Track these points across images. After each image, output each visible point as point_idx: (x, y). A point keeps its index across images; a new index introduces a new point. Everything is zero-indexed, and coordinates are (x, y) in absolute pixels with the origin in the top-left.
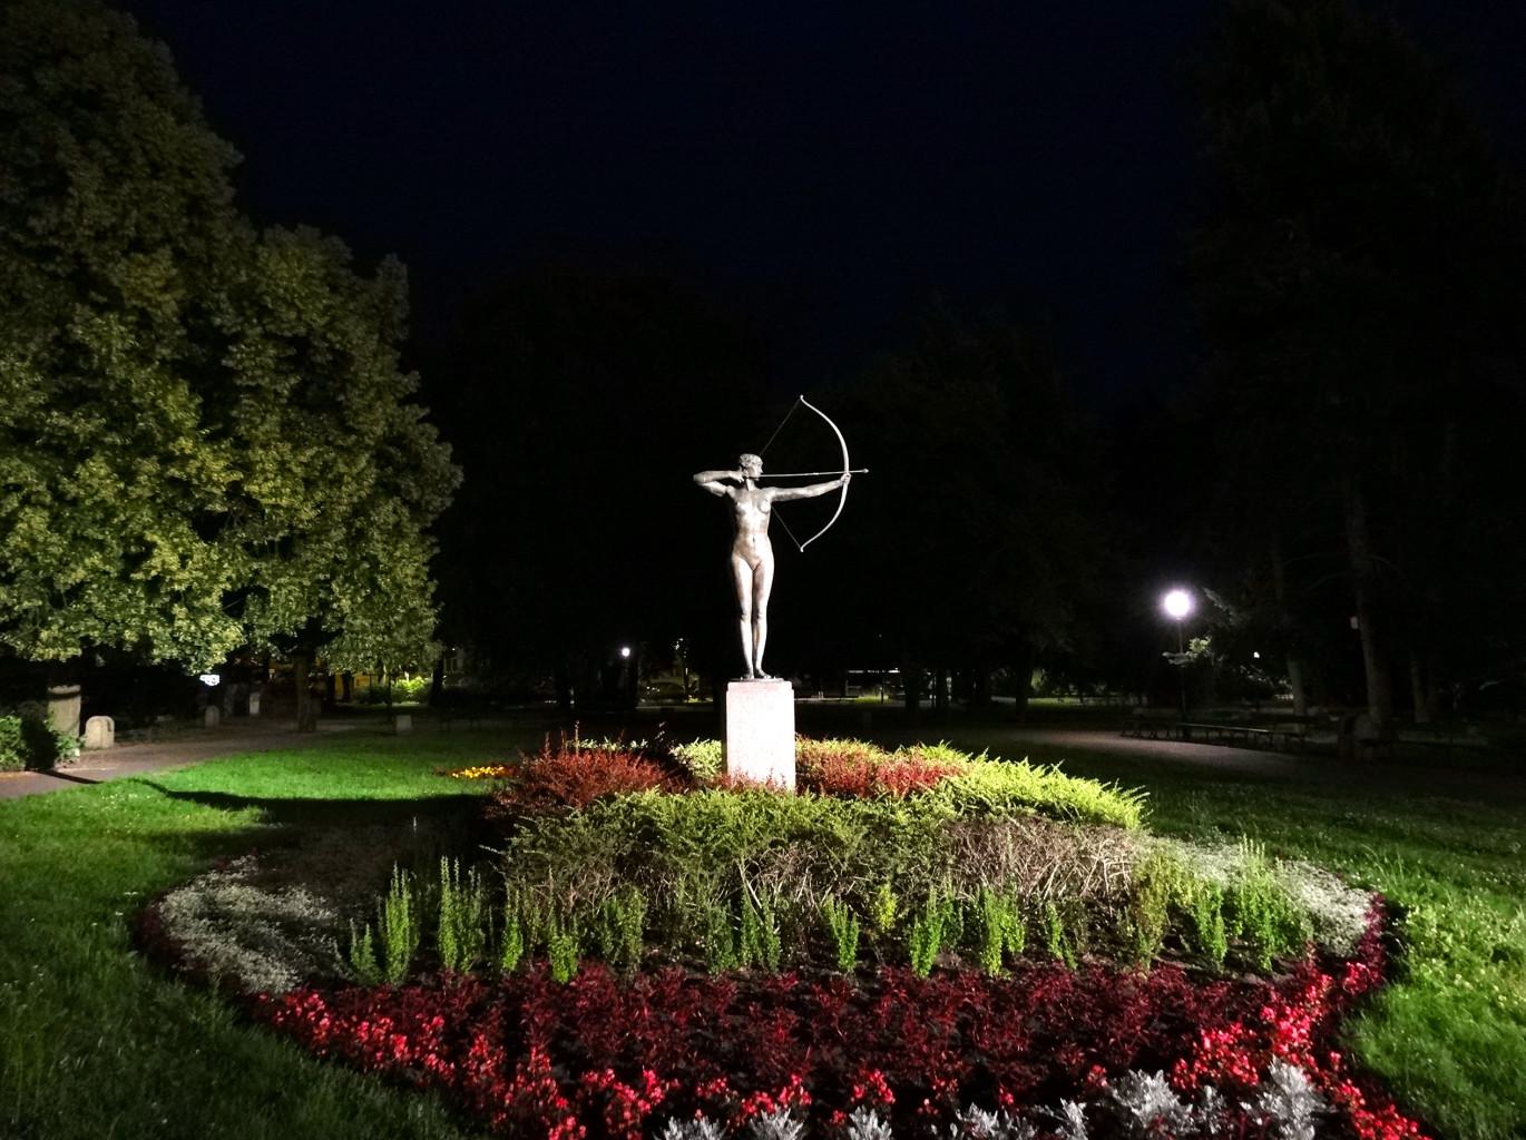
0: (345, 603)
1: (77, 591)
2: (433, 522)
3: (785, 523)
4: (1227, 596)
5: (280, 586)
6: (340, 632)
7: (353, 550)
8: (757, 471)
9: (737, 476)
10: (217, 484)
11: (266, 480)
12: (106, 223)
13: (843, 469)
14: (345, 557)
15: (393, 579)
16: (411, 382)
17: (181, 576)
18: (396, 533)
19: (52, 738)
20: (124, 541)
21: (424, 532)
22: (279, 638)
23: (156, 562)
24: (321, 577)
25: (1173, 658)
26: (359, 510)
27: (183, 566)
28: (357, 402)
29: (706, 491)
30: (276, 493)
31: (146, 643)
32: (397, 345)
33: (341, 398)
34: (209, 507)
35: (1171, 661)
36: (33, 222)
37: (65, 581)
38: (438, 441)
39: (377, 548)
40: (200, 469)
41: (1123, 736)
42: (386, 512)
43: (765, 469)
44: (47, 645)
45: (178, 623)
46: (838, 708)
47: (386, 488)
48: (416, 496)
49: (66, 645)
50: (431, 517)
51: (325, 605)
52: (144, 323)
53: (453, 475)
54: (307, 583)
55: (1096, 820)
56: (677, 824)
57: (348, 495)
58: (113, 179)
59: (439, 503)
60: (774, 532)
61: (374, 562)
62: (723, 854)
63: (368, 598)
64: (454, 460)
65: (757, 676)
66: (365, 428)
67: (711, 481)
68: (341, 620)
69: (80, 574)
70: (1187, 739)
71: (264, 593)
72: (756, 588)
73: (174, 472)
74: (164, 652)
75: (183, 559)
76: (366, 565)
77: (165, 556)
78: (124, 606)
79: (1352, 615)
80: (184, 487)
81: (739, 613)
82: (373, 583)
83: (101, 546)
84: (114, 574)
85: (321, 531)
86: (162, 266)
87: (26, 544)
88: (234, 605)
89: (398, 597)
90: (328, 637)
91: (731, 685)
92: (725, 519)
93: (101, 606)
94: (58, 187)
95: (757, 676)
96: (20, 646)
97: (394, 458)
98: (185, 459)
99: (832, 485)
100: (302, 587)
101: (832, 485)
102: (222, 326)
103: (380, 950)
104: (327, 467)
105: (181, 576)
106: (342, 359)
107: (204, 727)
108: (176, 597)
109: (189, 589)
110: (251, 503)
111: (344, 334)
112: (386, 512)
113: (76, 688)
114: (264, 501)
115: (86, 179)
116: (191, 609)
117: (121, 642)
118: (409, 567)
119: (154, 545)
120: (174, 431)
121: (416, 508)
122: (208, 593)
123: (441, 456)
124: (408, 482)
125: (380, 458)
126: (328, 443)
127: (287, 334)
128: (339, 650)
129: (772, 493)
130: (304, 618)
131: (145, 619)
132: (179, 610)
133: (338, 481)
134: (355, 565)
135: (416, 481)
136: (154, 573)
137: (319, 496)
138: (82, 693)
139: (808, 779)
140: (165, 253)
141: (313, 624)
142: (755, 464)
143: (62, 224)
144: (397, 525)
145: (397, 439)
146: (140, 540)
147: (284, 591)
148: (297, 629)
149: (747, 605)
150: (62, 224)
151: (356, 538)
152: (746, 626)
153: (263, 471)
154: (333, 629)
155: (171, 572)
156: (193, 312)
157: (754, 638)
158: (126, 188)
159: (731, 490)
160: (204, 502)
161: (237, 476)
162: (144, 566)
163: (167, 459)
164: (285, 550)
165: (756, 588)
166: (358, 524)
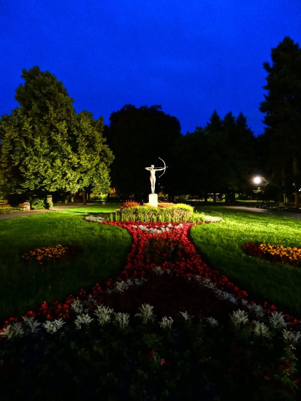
0: (96, 181)
1: (55, 181)
2: (110, 165)
3: (157, 174)
4: (266, 179)
5: (85, 178)
6: (95, 186)
7: (96, 172)
8: (153, 167)
9: (150, 168)
10: (76, 162)
11: (83, 161)
12: (55, 117)
13: (164, 167)
14: (95, 173)
15: (103, 177)
16: (105, 140)
17: (71, 178)
18: (104, 168)
19: (48, 204)
20: (62, 172)
21: (108, 167)
22: (85, 188)
23: (68, 176)
24: (92, 177)
25: (255, 191)
26: (98, 165)
27: (71, 176)
28: (97, 146)
29: (147, 170)
30: (85, 163)
31: (66, 188)
32: (102, 132)
33: (94, 145)
34: (75, 166)
35: (255, 192)
36: (44, 118)
37: (54, 179)
38: (110, 151)
39: (101, 172)
40: (74, 160)
41: (246, 207)
42: (102, 165)
43: (155, 167)
44: (52, 189)
45: (71, 185)
46: (199, 202)
47: (102, 160)
48: (106, 161)
49: (54, 189)
50: (109, 165)
51: (92, 182)
52: (62, 134)
53: (113, 157)
54: (89, 178)
55: (186, 210)
56: (140, 209)
57: (96, 162)
58: (55, 108)
59: (110, 162)
60: (156, 175)
61: (100, 174)
62: (144, 212)
63: (99, 180)
64: (113, 154)
65: (153, 193)
66: (98, 150)
67: (147, 169)
68: (95, 184)
69: (56, 178)
70: (257, 207)
71: (82, 180)
72: (153, 182)
73: (70, 161)
74: (68, 190)
75: (72, 175)
76: (99, 174)
77: (69, 175)
78: (62, 183)
79: (294, 183)
80: (71, 163)
81: (151, 186)
82: (100, 178)
83: (58, 173)
84: (61, 177)
85: (91, 168)
86: (64, 124)
87: (49, 174)
88: (78, 182)
89: (104, 180)
90: (93, 187)
91: (150, 195)
92: (149, 173)
93: (59, 183)
94: (46, 110)
95: (153, 193)
96: (48, 189)
97: (103, 155)
98: (71, 159)
99: (163, 169)
100: (88, 178)
101: (163, 169)
102: (75, 134)
103: (110, 219)
104: (92, 158)
105: (71, 178)
106: (94, 138)
107: (65, 204)
108: (70, 181)
109: (72, 180)
110: (81, 165)
111: (94, 134)
112: (102, 165)
113: (51, 196)
114: (83, 165)
115: (51, 109)
116: (72, 183)
117: (62, 188)
118: (106, 175)
119: (67, 173)
120: (69, 154)
121: (106, 163)
122: (75, 180)
123: (110, 153)
124: (105, 159)
125: (100, 155)
126: (92, 153)
127: (86, 135)
128: (95, 189)
129: (155, 170)
130: (89, 184)
131: (66, 184)
132: (71, 183)
133: (94, 160)
134: (97, 175)
135: (106, 158)
136: (67, 178)
137: (91, 163)
138: (52, 196)
139: (158, 205)
140: (64, 122)
141: (90, 185)
142: (153, 166)
143: (48, 118)
144: (104, 167)
145: (103, 151)
146: (65, 172)
147: (86, 179)
148: (88, 186)
149: (152, 185)
150: (48, 118)
151: (97, 170)
152: (152, 187)
153: (83, 160)
154: (94, 186)
155: (70, 177)
156: (69, 131)
157: (153, 189)
158: (58, 110)
159: (150, 170)
160: (74, 165)
161: (79, 161)
162: (66, 176)
163: (69, 159)
164: (85, 172)
165: (153, 182)
166: (97, 167)
